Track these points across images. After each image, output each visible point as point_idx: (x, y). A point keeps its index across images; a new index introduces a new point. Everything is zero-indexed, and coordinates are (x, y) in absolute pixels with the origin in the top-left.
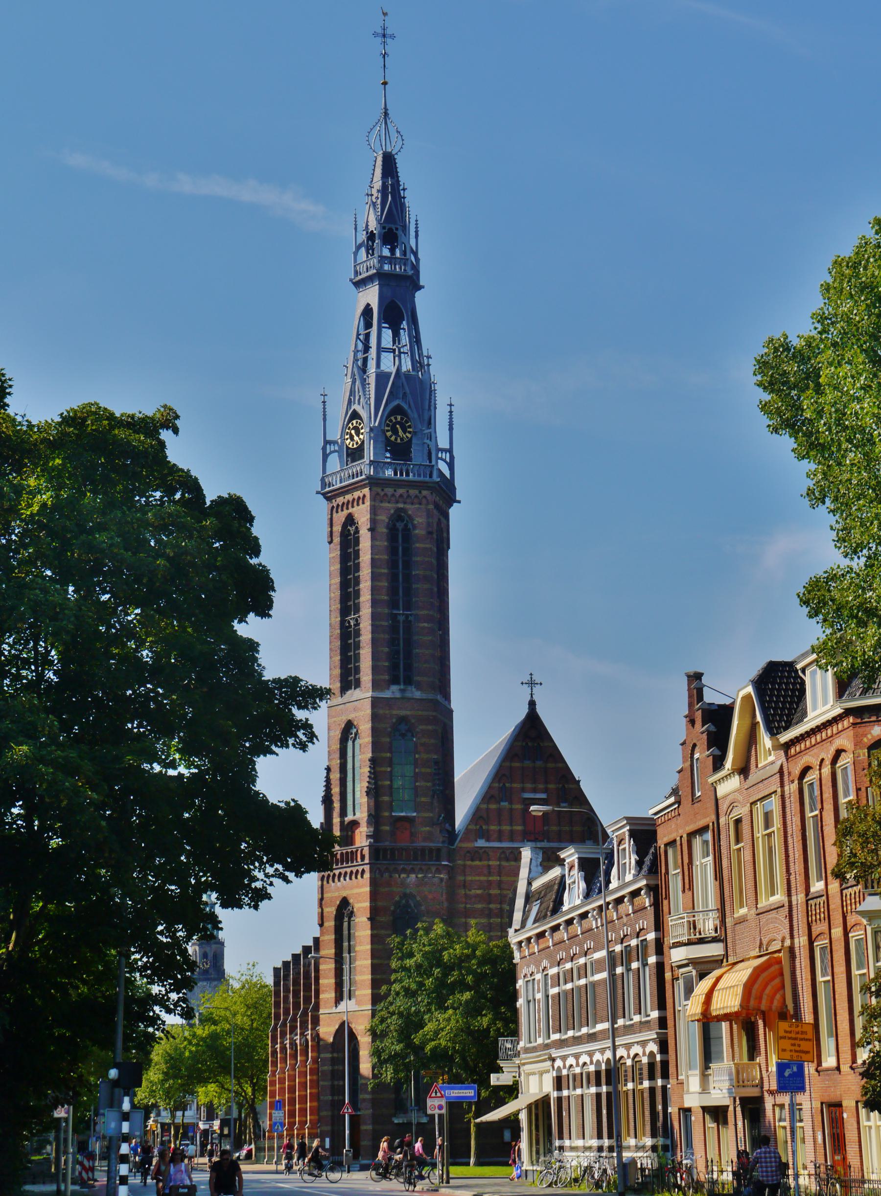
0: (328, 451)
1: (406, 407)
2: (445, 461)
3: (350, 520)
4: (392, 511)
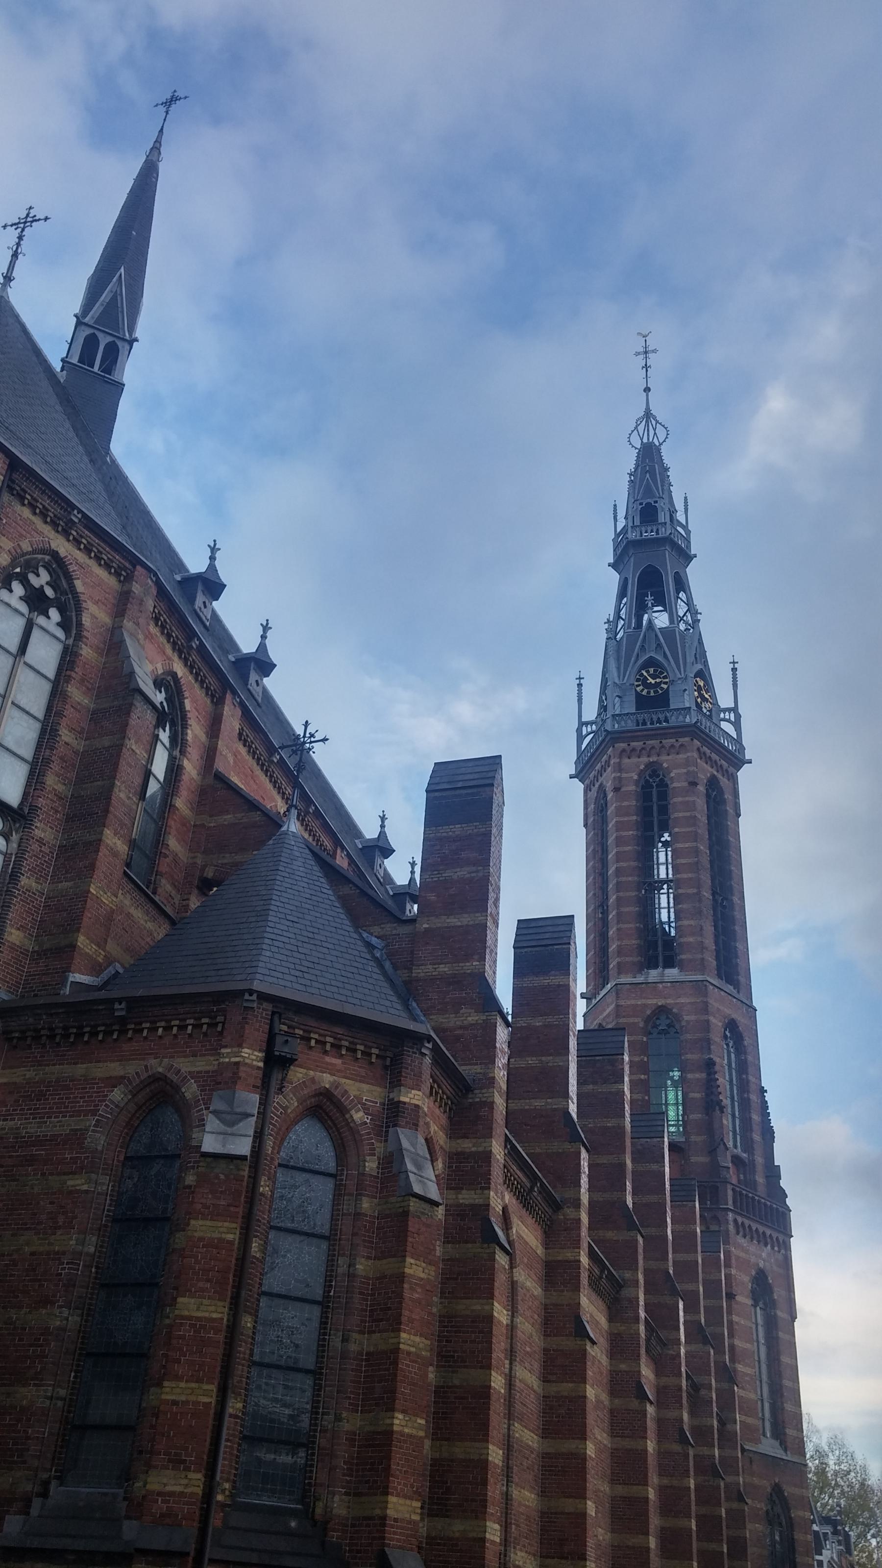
0: (584, 733)
1: (660, 658)
2: (729, 721)
3: (602, 790)
4: (642, 767)
